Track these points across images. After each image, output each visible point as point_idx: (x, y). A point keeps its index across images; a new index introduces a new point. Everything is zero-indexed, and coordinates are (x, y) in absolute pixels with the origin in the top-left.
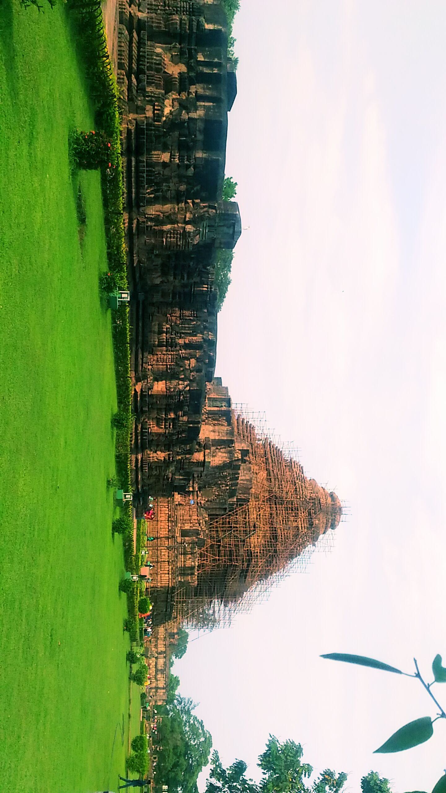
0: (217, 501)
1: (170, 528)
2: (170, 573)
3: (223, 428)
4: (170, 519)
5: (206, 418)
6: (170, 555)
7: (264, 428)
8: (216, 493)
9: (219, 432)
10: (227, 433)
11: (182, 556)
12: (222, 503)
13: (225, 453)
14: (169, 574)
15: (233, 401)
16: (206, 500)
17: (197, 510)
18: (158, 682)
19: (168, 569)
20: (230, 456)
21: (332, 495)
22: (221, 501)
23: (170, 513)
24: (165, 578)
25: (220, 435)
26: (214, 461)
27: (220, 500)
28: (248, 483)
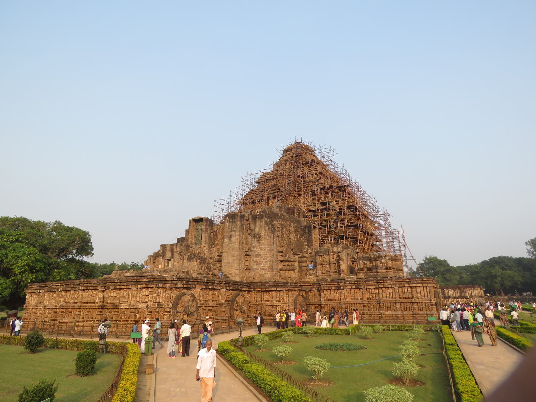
0: (307, 235)
1: (354, 287)
2: (415, 285)
3: (226, 229)
4: (342, 288)
5: (215, 247)
6: (390, 286)
7: (230, 202)
8: (298, 237)
9: (232, 231)
10: (233, 222)
11: (378, 271)
12: (309, 231)
13: (255, 224)
14: (416, 287)
15: (196, 216)
16: (307, 247)
17: (321, 256)
18: (473, 295)
19: (409, 289)
20: (259, 217)
21: (286, 151)
22: (307, 231)
23: (333, 288)
24: (422, 292)
25: (234, 229)
26: (265, 235)
27: (306, 233)
28: (283, 209)
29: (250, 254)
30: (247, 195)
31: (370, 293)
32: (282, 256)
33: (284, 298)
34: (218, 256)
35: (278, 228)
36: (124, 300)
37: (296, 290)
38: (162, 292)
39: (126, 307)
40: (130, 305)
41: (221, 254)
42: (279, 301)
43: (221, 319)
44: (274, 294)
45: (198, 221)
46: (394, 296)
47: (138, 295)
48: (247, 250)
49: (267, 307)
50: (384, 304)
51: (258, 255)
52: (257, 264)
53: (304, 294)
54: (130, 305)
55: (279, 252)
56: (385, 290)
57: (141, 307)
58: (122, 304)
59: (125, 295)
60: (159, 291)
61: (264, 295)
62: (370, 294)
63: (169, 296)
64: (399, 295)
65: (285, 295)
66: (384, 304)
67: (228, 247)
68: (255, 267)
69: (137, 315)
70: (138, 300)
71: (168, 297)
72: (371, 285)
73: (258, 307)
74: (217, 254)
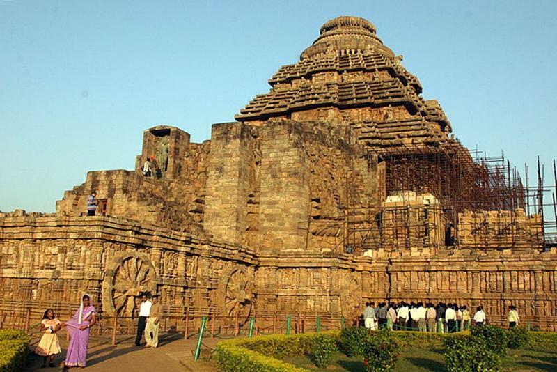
29: (257, 201)
30: (251, 104)
31: (487, 280)
32: (316, 207)
33: (323, 282)
34: (197, 201)
35: (312, 155)
36: (9, 262)
37: (345, 269)
38: (83, 249)
39: (13, 276)
40: (21, 272)
41: (202, 198)
42: (312, 287)
43: (200, 311)
44: (303, 272)
45: (162, 132)
46: (533, 287)
47: (37, 253)
48: (251, 193)
49: (289, 298)
50: (513, 301)
51: (272, 204)
52: (270, 221)
53: (359, 278)
54: (21, 272)
55: (313, 200)
56: (516, 275)
57: (42, 277)
58: (5, 270)
59: (11, 251)
60: (79, 246)
61: (282, 275)
62: (486, 281)
63: (98, 256)
64: (544, 287)
65: (324, 276)
66: (513, 301)
67: (216, 185)
68: (266, 224)
69: (35, 291)
70: (36, 263)
71: (96, 258)
72: (490, 266)
73: (271, 297)
74: (195, 198)
